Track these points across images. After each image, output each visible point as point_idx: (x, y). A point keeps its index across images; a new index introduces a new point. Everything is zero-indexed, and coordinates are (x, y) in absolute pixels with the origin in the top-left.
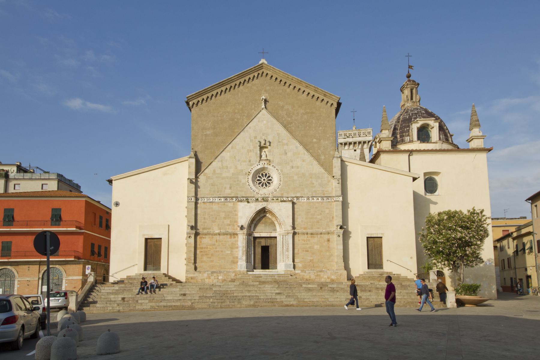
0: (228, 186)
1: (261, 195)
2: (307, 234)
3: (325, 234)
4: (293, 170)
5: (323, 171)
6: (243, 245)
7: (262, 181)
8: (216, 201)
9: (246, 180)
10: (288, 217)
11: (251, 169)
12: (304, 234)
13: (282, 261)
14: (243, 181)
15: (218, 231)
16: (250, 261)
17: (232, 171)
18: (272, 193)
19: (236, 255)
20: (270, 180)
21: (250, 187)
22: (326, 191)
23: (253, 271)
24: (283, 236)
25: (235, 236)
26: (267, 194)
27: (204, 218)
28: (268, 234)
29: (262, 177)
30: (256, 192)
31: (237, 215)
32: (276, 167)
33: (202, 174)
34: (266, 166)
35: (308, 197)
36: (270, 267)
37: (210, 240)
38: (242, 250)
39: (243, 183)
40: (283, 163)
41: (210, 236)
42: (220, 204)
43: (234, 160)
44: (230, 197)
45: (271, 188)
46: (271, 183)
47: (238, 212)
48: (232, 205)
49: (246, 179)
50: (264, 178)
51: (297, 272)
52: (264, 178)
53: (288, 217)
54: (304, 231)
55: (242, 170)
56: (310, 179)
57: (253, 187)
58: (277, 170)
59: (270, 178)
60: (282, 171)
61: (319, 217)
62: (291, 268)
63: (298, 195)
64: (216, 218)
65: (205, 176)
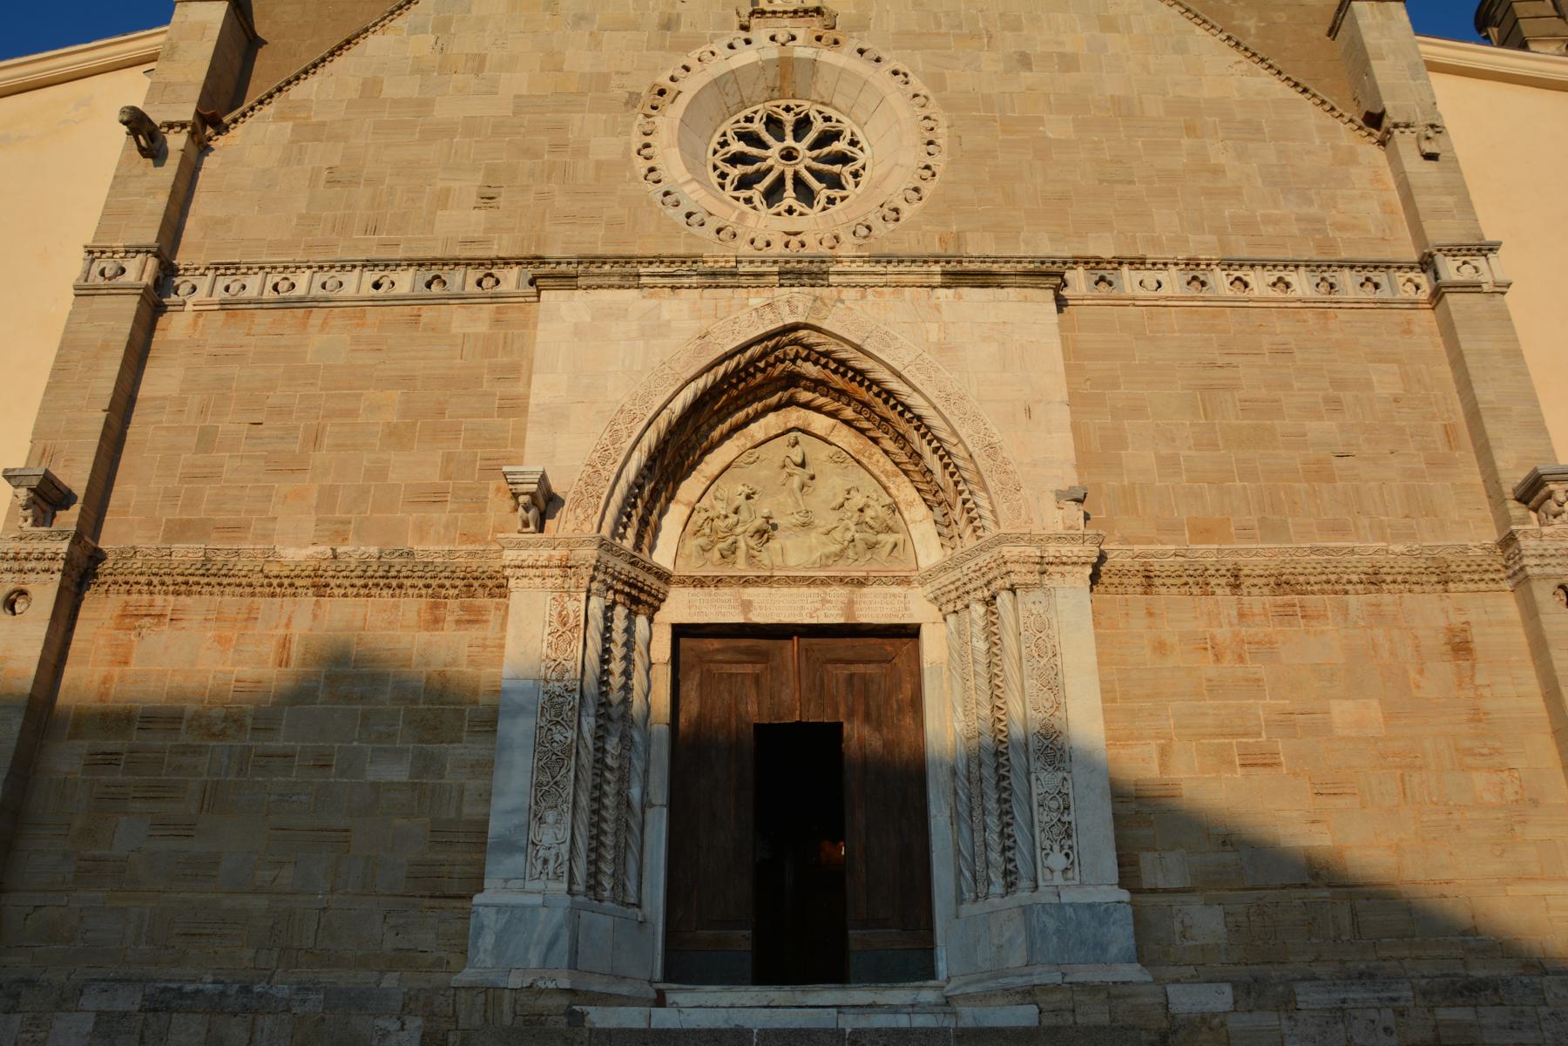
0: (468, 186)
1: (760, 243)
2: (1236, 581)
3: (1409, 581)
4: (1027, 77)
5: (1280, 89)
7: (770, 162)
8: (342, 293)
9: (628, 145)
10: (1029, 411)
11: (679, 73)
12: (1198, 580)
14: (605, 147)
15: (311, 550)
16: (618, 884)
17: (516, 83)
19: (470, 811)
20: (844, 159)
21: (662, 187)
22: (1342, 227)
23: (660, 1001)
24: (990, 602)
25: (482, 601)
26: (811, 240)
27: (207, 440)
28: (824, 601)
29: (767, 137)
31: (516, 407)
32: (883, 55)
33: (268, 110)
34: (802, 51)
35: (1192, 263)
37: (220, 640)
39: (599, 165)
40: (946, 34)
41: (230, 602)
42: (373, 315)
43: (548, 15)
44: (468, 263)
45: (857, 201)
47: (529, 384)
48: (483, 328)
49: (628, 134)
50: (789, 141)
51: (1190, 999)
52: (802, 147)
53: (1029, 411)
54: (1206, 553)
55: (602, 81)
56: (1186, 142)
57: (687, 189)
58: (901, 77)
59: (840, 146)
60: (937, 82)
61: (1323, 428)
62: (1114, 950)
63: (1092, 251)
64: (316, 440)
65: (290, 125)
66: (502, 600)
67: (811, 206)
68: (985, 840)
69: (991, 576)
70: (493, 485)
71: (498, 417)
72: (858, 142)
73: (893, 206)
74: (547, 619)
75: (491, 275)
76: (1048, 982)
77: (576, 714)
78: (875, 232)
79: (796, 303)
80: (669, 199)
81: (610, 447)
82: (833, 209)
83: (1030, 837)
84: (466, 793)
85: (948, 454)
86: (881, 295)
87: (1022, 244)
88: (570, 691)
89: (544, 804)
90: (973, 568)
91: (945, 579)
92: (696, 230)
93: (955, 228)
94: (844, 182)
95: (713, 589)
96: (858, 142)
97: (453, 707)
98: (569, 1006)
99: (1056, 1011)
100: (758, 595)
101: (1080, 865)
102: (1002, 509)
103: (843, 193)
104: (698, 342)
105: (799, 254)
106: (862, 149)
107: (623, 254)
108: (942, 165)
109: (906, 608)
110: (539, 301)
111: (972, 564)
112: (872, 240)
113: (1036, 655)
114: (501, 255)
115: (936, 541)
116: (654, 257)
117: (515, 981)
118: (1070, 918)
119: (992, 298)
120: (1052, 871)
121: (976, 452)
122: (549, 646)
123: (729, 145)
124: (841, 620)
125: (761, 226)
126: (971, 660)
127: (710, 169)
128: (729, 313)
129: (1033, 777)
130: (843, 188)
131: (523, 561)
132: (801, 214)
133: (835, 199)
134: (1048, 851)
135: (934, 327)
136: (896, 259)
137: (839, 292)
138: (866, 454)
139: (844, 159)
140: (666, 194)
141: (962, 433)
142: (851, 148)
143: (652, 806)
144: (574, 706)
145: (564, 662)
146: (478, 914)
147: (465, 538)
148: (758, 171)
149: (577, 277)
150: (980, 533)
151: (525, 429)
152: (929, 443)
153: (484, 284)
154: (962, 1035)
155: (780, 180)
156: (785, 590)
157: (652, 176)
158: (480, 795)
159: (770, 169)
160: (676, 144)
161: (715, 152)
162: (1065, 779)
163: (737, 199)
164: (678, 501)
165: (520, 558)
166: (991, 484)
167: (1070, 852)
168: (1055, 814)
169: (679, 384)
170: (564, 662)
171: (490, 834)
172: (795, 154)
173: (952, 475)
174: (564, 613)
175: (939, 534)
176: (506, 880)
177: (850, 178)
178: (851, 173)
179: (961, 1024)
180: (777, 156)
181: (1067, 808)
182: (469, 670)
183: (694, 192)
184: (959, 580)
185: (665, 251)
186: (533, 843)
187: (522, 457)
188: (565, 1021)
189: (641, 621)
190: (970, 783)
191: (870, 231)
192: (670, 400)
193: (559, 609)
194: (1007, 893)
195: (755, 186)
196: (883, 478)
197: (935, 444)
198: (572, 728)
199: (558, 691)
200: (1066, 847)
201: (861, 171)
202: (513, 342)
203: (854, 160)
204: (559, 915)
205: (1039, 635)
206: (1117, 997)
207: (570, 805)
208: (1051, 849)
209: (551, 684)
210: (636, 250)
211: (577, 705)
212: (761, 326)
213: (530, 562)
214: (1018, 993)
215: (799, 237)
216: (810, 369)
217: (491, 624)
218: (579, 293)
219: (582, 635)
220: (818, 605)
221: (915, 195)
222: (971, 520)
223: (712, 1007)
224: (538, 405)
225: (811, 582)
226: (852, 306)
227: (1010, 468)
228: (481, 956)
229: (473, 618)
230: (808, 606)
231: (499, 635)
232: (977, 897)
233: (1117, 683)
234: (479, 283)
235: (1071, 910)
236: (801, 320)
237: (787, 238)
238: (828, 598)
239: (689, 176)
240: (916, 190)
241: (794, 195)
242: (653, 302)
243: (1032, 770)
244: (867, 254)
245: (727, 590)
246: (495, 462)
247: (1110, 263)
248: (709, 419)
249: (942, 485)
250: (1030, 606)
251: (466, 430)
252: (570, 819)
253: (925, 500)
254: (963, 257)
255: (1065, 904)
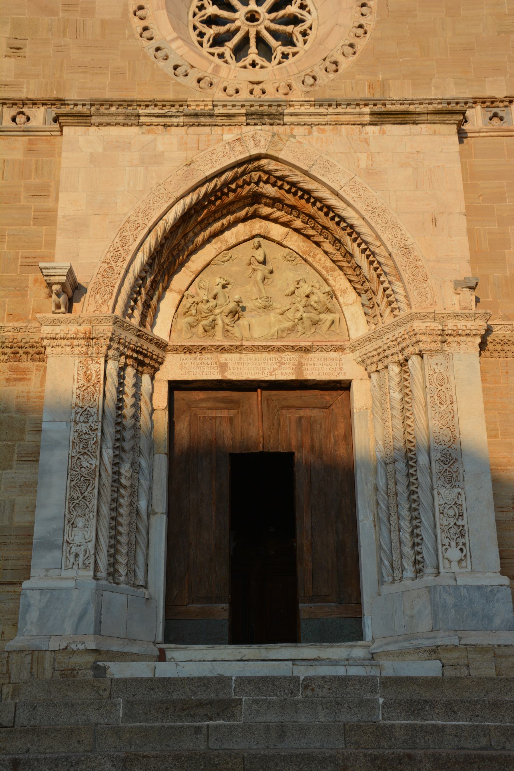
1: (231, 90)
6: (83, 427)
7: (237, 23)
10: (435, 221)
13: (408, 565)
16: (132, 572)
18: (311, 81)
19: (19, 519)
20: (295, 20)
21: (154, 44)
23: (162, 657)
24: (404, 363)
25: (26, 364)
26: (270, 88)
28: (280, 364)
30: (194, 75)
36: (304, 628)
38: (71, 469)
39: (104, 23)
46: (298, 39)
47: (57, 199)
48: (18, 155)
57: (174, 45)
62: (497, 621)
63: (489, 92)
66: (41, 363)
67: (270, 60)
68: (399, 538)
69: (404, 344)
70: (31, 277)
71: (34, 225)
72: (306, 6)
73: (333, 59)
74: (76, 377)
75: (23, 113)
76: (449, 644)
77: (99, 447)
78: (319, 81)
79: (258, 137)
80: (159, 54)
81: (120, 248)
82: (286, 62)
83: (434, 536)
84: (16, 506)
85: (373, 253)
86: (323, 131)
87: (432, 88)
88: (94, 430)
89: (75, 513)
90: (391, 339)
91: (370, 347)
92: (181, 79)
93: (381, 76)
94: (295, 40)
95: (198, 355)
96: (306, 6)
97: (5, 443)
98: (95, 662)
99: (455, 666)
100: (232, 359)
101: (471, 557)
102: (414, 294)
103: (295, 50)
104: (185, 168)
105: (262, 99)
106: (309, 12)
107: (126, 98)
108: (372, 24)
109: (341, 369)
110: (62, 135)
111: (390, 336)
112: (317, 88)
113: (438, 403)
114: (30, 96)
115: (363, 319)
116: (150, 101)
117: (54, 645)
118: (464, 596)
119: (409, 132)
120: (450, 562)
121: (394, 251)
122: (78, 396)
123: (205, 8)
124: (293, 378)
125: (231, 76)
126: (389, 407)
127: (191, 29)
128: (208, 146)
129: (436, 492)
130: (294, 45)
131: (57, 334)
132: (262, 67)
133: (288, 54)
134: (447, 547)
135: (363, 157)
136: (334, 103)
137: (292, 130)
138: (311, 254)
139: (295, 20)
140: (158, 49)
141: (384, 237)
142: (301, 11)
143: (155, 513)
144: (97, 441)
145: (88, 409)
146: (26, 596)
147: (11, 317)
148: (228, 31)
149: (91, 116)
150: (396, 312)
151: (55, 235)
152: (359, 245)
153: (17, 120)
154: (386, 682)
155: (246, 39)
156: (251, 355)
157: (146, 34)
158: (27, 508)
159: (237, 30)
160: (164, 6)
161: (195, 15)
162: (459, 494)
163: (213, 54)
164: (172, 290)
165: (54, 332)
166: (405, 276)
167: (463, 547)
168: (452, 520)
169: (171, 201)
170: (88, 409)
171: (35, 536)
172: (257, 16)
173: (376, 269)
174: (89, 372)
175: (366, 314)
176: (47, 570)
177: (300, 37)
178: (301, 32)
179: (384, 674)
180: (243, 18)
181: (461, 515)
182: (17, 415)
183: (179, 48)
184: (380, 347)
185: (158, 96)
186: (67, 542)
187: (54, 256)
188: (92, 673)
189: (146, 379)
190: (388, 496)
191: (315, 80)
192: (165, 213)
193: (85, 370)
194: (416, 577)
195: (226, 44)
196: (324, 273)
197: (363, 246)
198: (96, 458)
199: (85, 430)
200: (461, 544)
201: (309, 31)
202: (43, 168)
203: (303, 21)
204: (87, 595)
205: (440, 388)
206: (501, 656)
207: (95, 514)
208: (449, 545)
209: (80, 425)
210: (136, 96)
211: (99, 441)
212: (233, 157)
213: (62, 335)
214: (425, 651)
215: (261, 86)
216: (269, 190)
217: (33, 382)
218: (93, 129)
219: (102, 389)
220: (276, 366)
221: (350, 50)
222: (390, 303)
223: (200, 661)
224: (64, 217)
225: (270, 349)
226: (301, 140)
227: (420, 263)
228: (28, 627)
229: (19, 376)
230: (269, 367)
231: (39, 390)
232: (394, 580)
233: (499, 423)
234: (14, 120)
235: (465, 590)
236: (263, 151)
237: (251, 86)
238: (283, 361)
239: (175, 35)
240: (351, 45)
241: (256, 51)
242: (150, 137)
243: (435, 486)
244: (313, 99)
245: (209, 356)
246: (33, 260)
247: (502, 101)
248: (194, 228)
249: (368, 277)
250: (434, 366)
251: (9, 235)
252: (95, 524)
253: (355, 288)
254: (386, 100)
255: (461, 586)
